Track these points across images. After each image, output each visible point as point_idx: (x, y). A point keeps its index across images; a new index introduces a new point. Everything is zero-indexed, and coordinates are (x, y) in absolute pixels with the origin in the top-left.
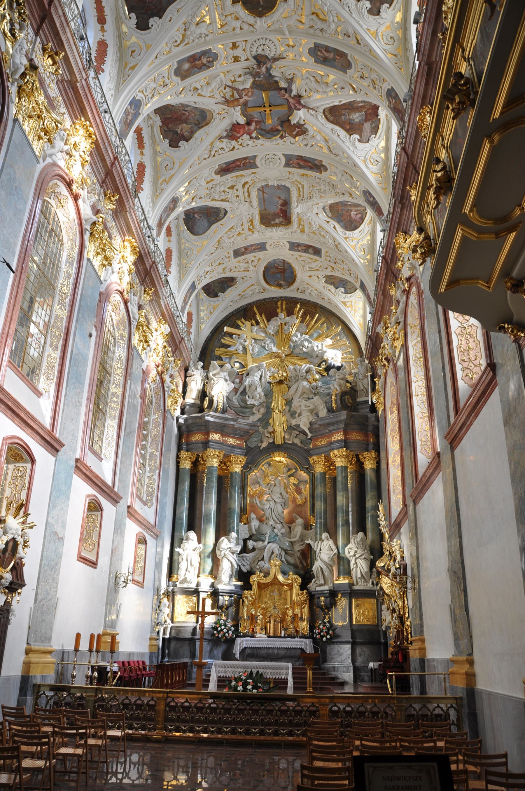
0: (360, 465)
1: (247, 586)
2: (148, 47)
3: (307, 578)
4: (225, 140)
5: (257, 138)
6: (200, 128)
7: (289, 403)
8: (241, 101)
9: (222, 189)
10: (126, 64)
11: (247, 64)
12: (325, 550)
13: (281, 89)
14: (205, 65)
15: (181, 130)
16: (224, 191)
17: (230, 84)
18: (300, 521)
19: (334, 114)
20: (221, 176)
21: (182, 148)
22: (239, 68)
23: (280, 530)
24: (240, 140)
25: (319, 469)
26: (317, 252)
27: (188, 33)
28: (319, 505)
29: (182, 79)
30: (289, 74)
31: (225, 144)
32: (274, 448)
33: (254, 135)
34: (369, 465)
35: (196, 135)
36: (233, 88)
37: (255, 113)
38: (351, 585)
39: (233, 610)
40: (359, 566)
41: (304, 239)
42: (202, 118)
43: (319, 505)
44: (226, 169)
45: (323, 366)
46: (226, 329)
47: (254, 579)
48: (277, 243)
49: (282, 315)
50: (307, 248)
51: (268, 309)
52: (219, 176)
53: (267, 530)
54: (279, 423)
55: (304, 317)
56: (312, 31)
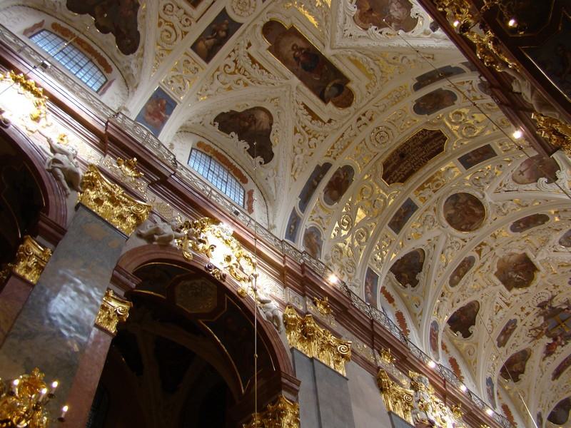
2: (477, 344)
4: (547, 358)
5: (566, 343)
6: (527, 360)
8: (544, 332)
9: (563, 386)
10: (470, 361)
11: (535, 311)
13: (564, 310)
14: (511, 330)
15: (516, 369)
16: (565, 386)
17: (531, 328)
20: (557, 379)
21: (523, 379)
24: (556, 352)
27: (494, 322)
29: (504, 346)
30: (563, 300)
31: (548, 360)
33: (563, 343)
35: (527, 366)
36: (534, 329)
37: (557, 332)
42: (524, 356)
44: (557, 374)
52: (556, 380)
56: (565, 274)
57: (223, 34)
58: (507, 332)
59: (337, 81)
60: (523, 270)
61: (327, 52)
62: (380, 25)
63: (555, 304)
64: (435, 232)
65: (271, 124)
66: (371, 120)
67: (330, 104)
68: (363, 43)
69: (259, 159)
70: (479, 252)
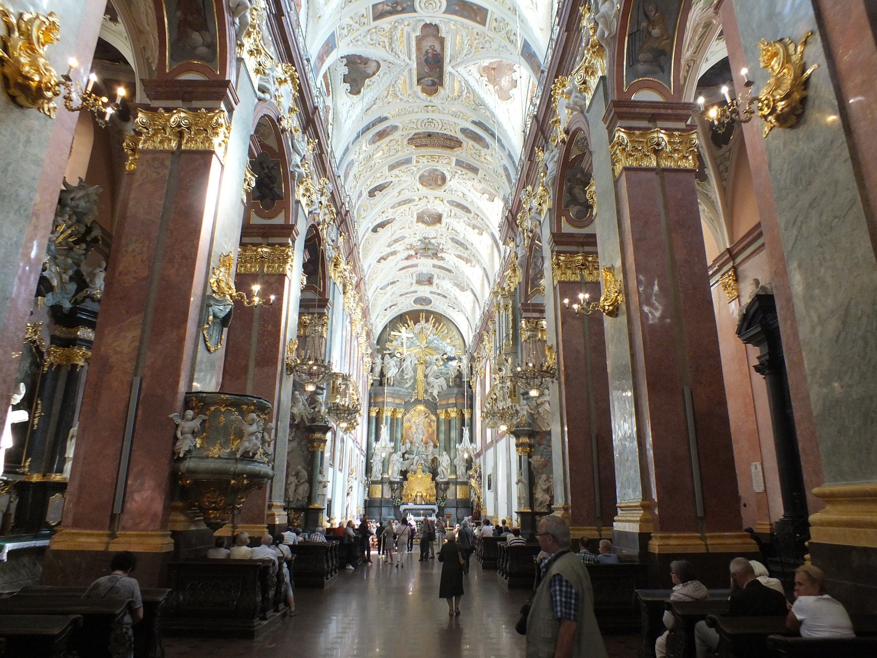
0: (463, 415)
1: (405, 479)
3: (434, 473)
7: (426, 376)
12: (444, 460)
18: (432, 444)
19: (459, 257)
22: (416, 239)
23: (422, 449)
25: (442, 417)
26: (445, 297)
28: (442, 436)
32: (418, 402)
34: (467, 416)
38: (456, 478)
39: (398, 491)
40: (461, 470)
41: (439, 292)
43: (442, 436)
45: (445, 357)
46: (392, 333)
47: (408, 475)
48: (424, 291)
49: (423, 322)
50: (439, 294)
51: (413, 317)
53: (415, 449)
54: (421, 387)
55: (435, 324)
57: (399, 8)
58: (396, 241)
59: (436, 80)
60: (433, 218)
61: (448, 68)
62: (489, 81)
63: (433, 241)
64: (409, 179)
65: (374, 74)
66: (433, 112)
67: (420, 87)
68: (472, 82)
69: (347, 86)
70: (420, 199)
